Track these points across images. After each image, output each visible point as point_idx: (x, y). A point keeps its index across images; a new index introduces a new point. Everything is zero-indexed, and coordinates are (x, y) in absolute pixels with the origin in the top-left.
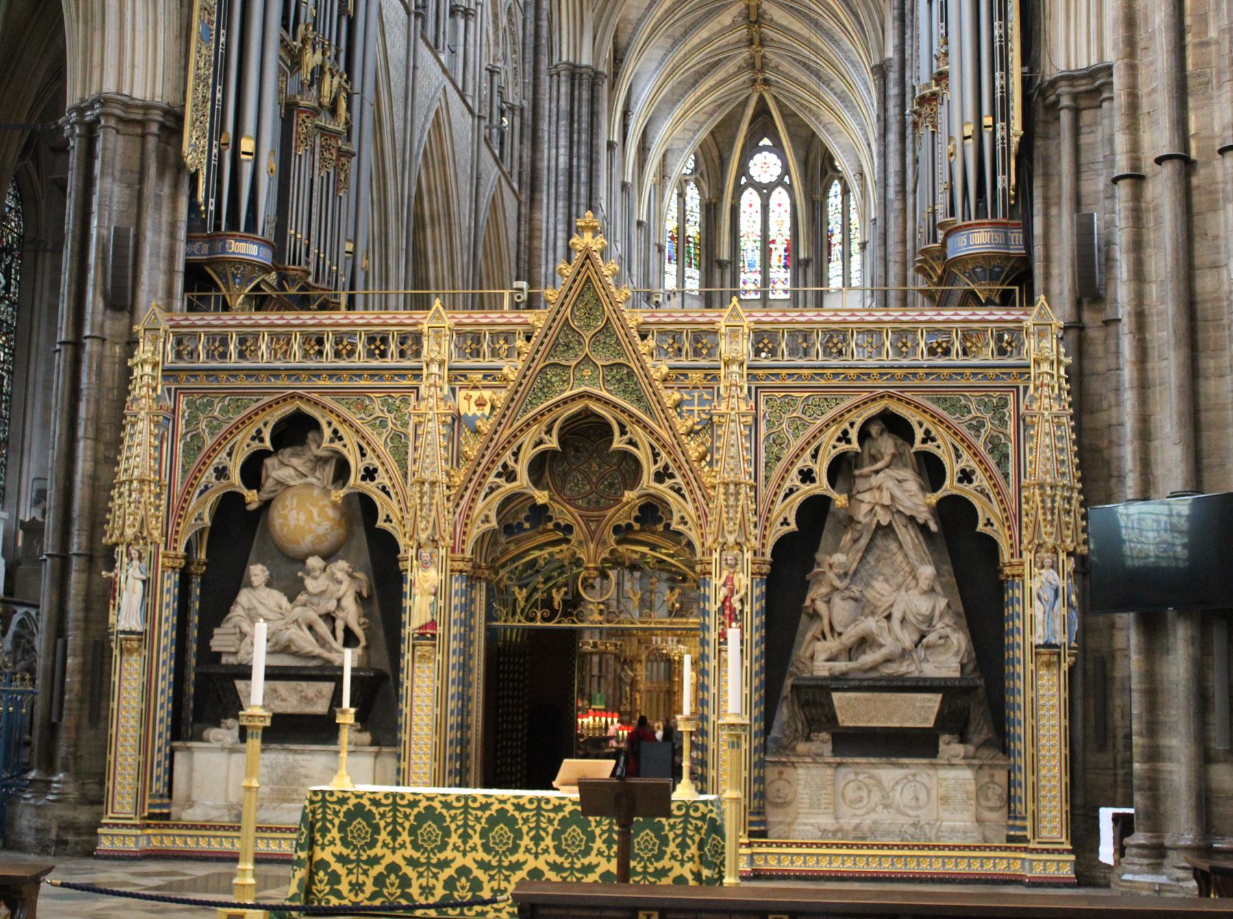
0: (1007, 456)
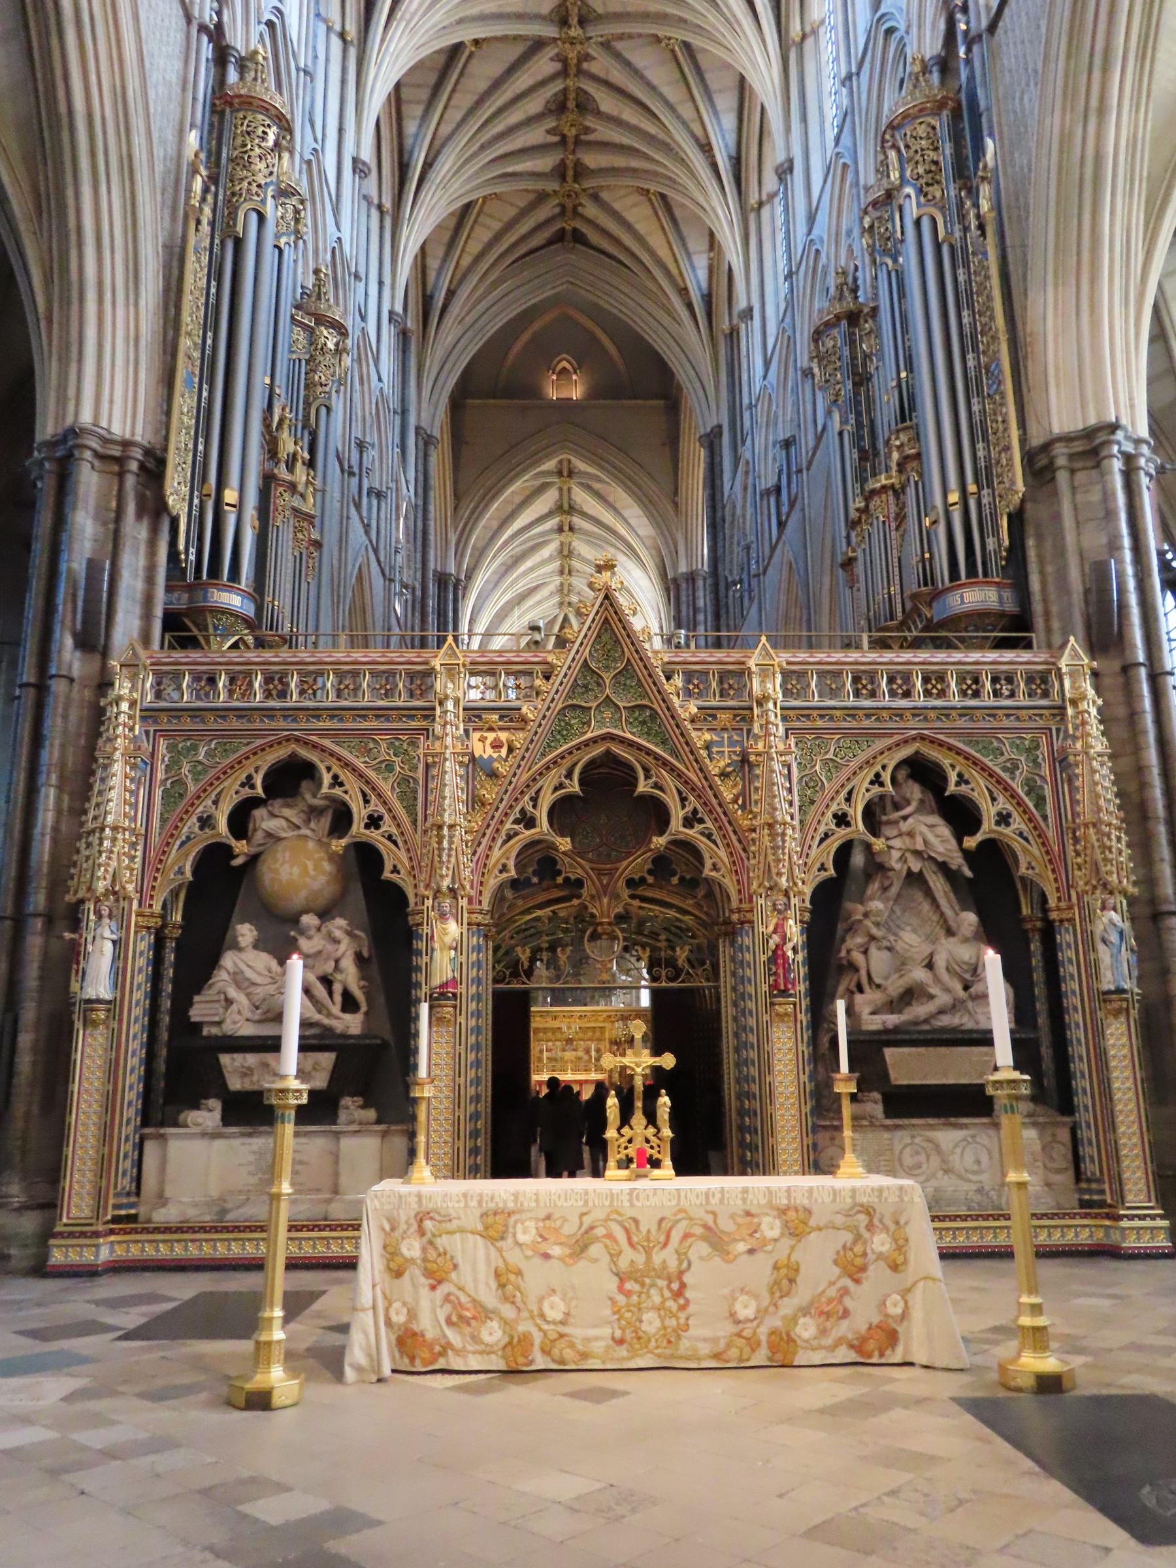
0: (1043, 798)
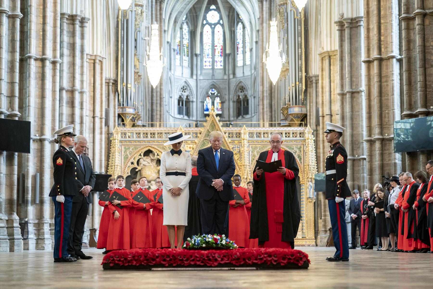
0: (301, 159)
